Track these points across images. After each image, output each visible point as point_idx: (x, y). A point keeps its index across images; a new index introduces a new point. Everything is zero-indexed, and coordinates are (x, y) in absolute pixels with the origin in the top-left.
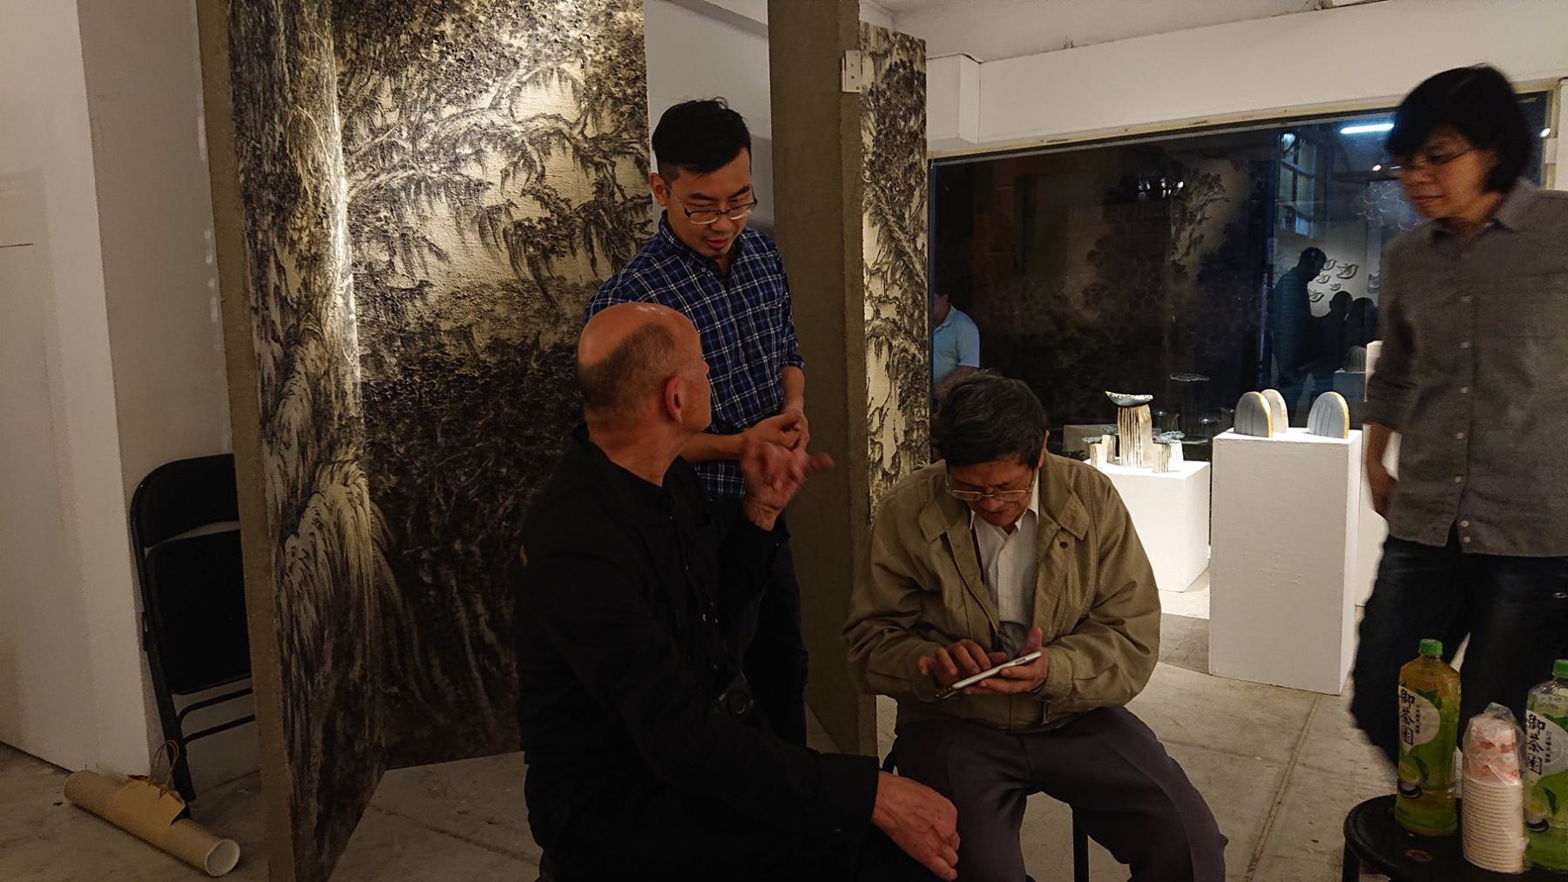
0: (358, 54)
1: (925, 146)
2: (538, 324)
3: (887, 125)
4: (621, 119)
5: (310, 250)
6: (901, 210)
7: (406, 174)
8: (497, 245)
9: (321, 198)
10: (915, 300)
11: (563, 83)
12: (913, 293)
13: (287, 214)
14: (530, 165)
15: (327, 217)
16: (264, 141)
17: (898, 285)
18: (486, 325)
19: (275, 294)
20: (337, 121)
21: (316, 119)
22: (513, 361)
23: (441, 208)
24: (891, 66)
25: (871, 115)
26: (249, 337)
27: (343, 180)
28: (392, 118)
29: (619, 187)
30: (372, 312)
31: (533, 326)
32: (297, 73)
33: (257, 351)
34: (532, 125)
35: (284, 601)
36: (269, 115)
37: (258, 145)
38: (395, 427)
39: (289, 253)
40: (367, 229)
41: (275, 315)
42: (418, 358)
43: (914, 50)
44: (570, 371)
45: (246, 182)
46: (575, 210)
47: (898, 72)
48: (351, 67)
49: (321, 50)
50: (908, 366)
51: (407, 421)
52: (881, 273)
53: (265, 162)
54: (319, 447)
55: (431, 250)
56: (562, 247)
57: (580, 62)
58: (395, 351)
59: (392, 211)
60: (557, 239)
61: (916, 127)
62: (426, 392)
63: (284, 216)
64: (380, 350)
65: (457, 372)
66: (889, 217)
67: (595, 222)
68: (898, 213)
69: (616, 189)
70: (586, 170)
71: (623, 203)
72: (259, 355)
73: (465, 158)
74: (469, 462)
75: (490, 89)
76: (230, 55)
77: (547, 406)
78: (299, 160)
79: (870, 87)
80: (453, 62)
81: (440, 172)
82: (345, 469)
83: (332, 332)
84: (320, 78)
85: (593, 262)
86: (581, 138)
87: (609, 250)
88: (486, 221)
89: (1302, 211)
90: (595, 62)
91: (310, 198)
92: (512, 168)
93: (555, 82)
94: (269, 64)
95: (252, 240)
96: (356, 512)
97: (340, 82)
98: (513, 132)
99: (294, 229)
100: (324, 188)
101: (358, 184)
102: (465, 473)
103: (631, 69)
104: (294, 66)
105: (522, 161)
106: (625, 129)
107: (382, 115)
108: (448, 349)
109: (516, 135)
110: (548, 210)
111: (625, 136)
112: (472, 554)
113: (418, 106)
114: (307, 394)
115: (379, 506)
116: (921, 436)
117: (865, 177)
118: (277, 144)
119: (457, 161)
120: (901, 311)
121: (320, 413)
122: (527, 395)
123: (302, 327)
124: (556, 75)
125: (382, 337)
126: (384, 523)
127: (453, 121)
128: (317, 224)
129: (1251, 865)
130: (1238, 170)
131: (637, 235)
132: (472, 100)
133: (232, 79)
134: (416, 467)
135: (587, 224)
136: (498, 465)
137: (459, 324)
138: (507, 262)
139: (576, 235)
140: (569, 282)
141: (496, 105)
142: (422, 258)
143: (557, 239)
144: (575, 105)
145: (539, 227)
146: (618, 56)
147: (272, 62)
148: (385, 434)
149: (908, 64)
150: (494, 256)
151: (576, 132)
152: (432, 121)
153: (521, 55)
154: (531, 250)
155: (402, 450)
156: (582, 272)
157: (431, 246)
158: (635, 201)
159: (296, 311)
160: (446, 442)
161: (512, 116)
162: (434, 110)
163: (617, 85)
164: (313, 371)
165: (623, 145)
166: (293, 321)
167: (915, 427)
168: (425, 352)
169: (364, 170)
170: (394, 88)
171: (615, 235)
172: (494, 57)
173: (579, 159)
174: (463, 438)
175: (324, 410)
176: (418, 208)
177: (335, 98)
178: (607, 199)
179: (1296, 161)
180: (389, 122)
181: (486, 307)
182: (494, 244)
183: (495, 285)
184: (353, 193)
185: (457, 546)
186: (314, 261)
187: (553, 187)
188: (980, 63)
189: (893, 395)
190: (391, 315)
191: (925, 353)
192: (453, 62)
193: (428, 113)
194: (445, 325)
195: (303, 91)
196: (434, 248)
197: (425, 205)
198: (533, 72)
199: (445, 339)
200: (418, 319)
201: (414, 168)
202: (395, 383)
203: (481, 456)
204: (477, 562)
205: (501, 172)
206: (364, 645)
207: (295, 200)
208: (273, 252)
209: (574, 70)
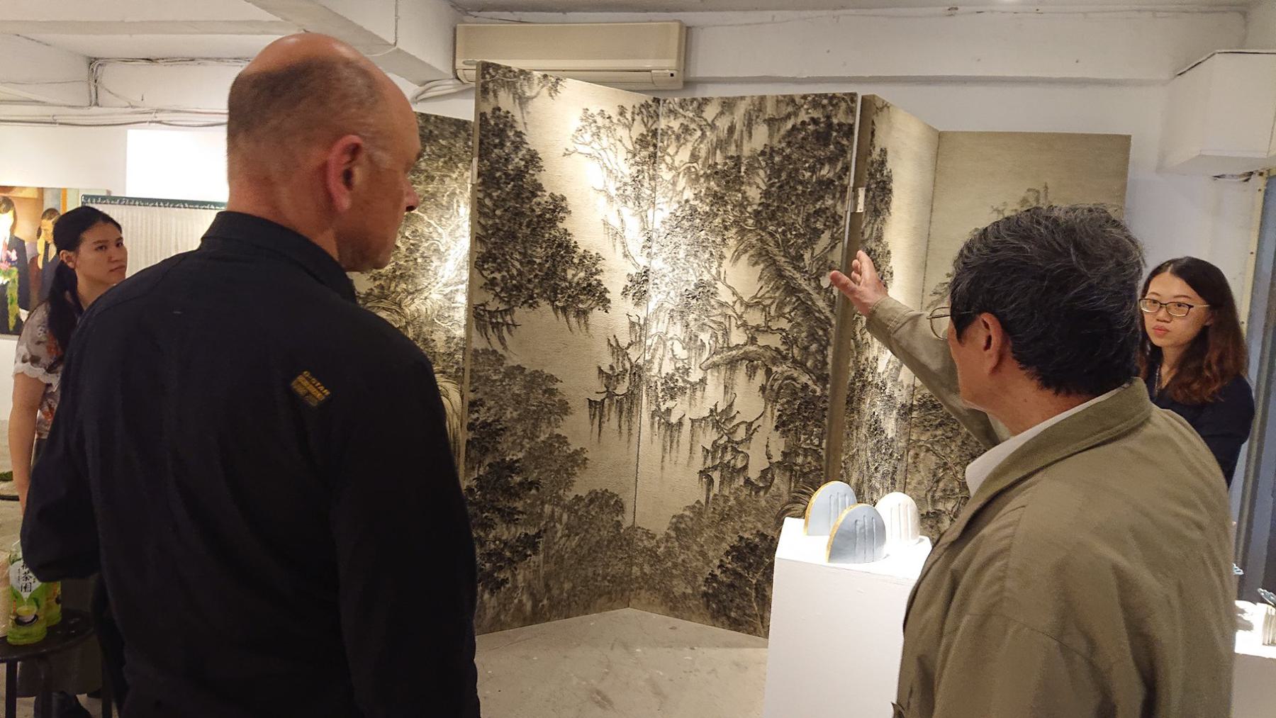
12: (811, 327)
17: (787, 318)
24: (794, 126)
25: (761, 172)
66: (778, 258)
149: (822, 120)
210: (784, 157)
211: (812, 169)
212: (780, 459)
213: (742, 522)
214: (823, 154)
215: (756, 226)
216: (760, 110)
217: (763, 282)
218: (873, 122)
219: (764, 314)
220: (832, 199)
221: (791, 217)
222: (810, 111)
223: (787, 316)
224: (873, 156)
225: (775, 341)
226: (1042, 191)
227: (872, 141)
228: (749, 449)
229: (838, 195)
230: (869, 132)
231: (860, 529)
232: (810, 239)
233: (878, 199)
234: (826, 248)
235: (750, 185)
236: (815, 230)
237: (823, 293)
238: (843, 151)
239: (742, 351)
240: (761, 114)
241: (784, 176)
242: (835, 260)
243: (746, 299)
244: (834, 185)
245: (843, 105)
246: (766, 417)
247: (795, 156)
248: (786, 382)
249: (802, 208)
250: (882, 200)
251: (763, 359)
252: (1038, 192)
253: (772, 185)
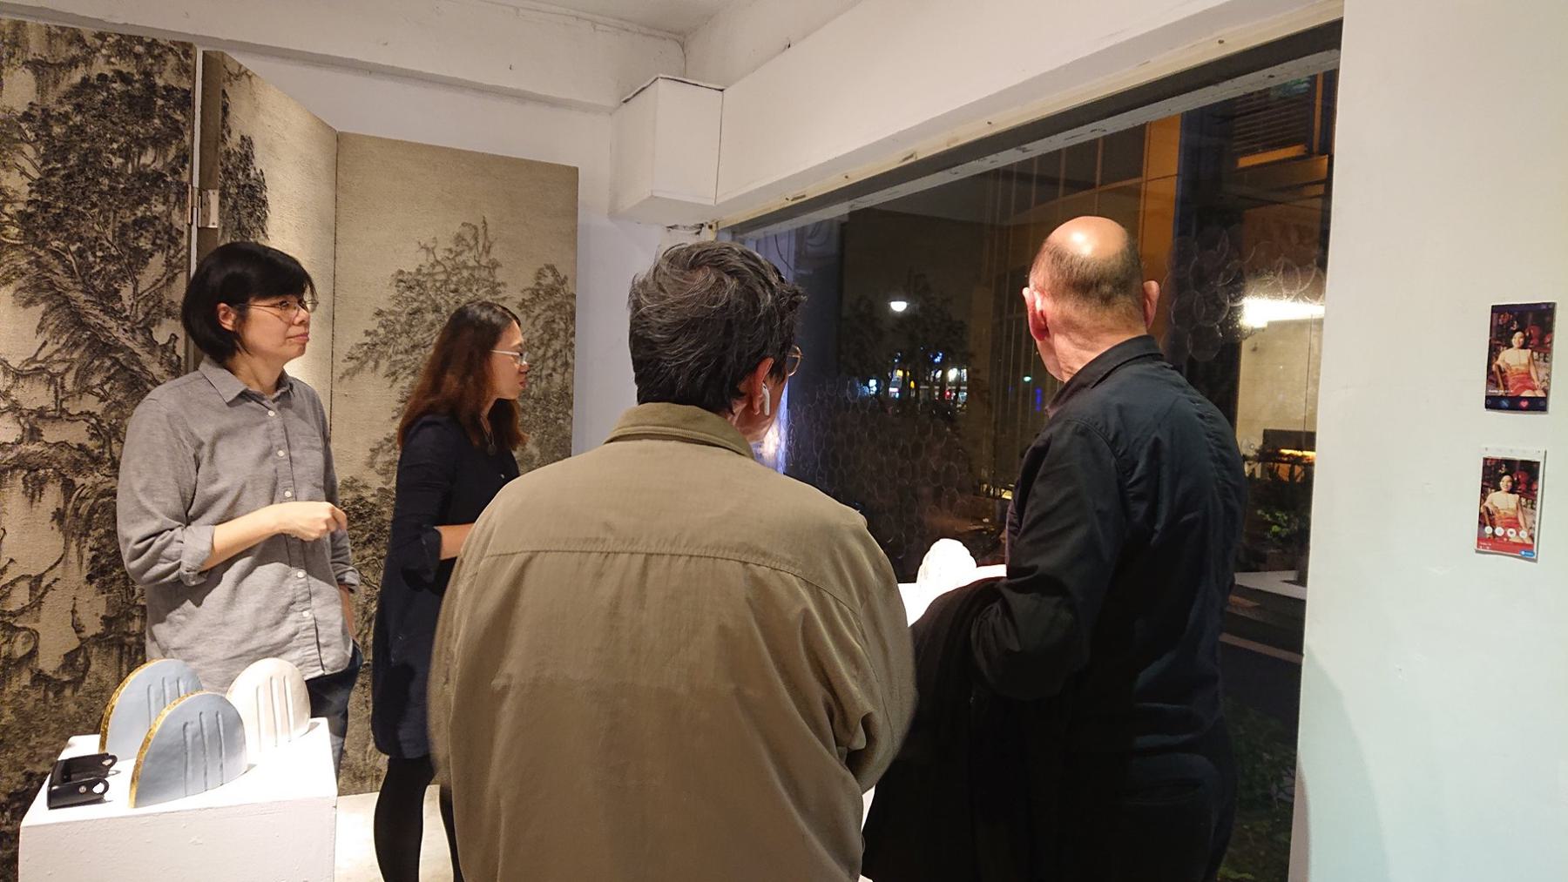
17: (98, 395)
24: (85, 81)
25: (28, 149)
47: (108, 90)
66: (74, 295)
149: (137, 77)
188: (722, 90)
210: (70, 127)
211: (125, 153)
212: (99, 629)
213: (30, 748)
214: (142, 131)
215: (25, 238)
216: (16, 45)
217: (47, 335)
218: (224, 91)
219: (52, 388)
220: (164, 204)
221: (91, 228)
223: (96, 390)
224: (229, 145)
225: (76, 434)
226: (480, 227)
227: (223, 120)
228: (37, 621)
229: (173, 198)
230: (218, 109)
231: (194, 737)
232: (129, 265)
233: (244, 212)
234: (158, 281)
236: (138, 251)
237: (159, 353)
238: (177, 131)
239: (11, 455)
240: (18, 52)
241: (73, 159)
242: (175, 301)
243: (15, 363)
244: (164, 181)
245: (172, 60)
246: (66, 563)
247: (91, 129)
248: (101, 501)
249: (112, 215)
250: (250, 215)
251: (55, 465)
252: (475, 228)
253: (51, 173)
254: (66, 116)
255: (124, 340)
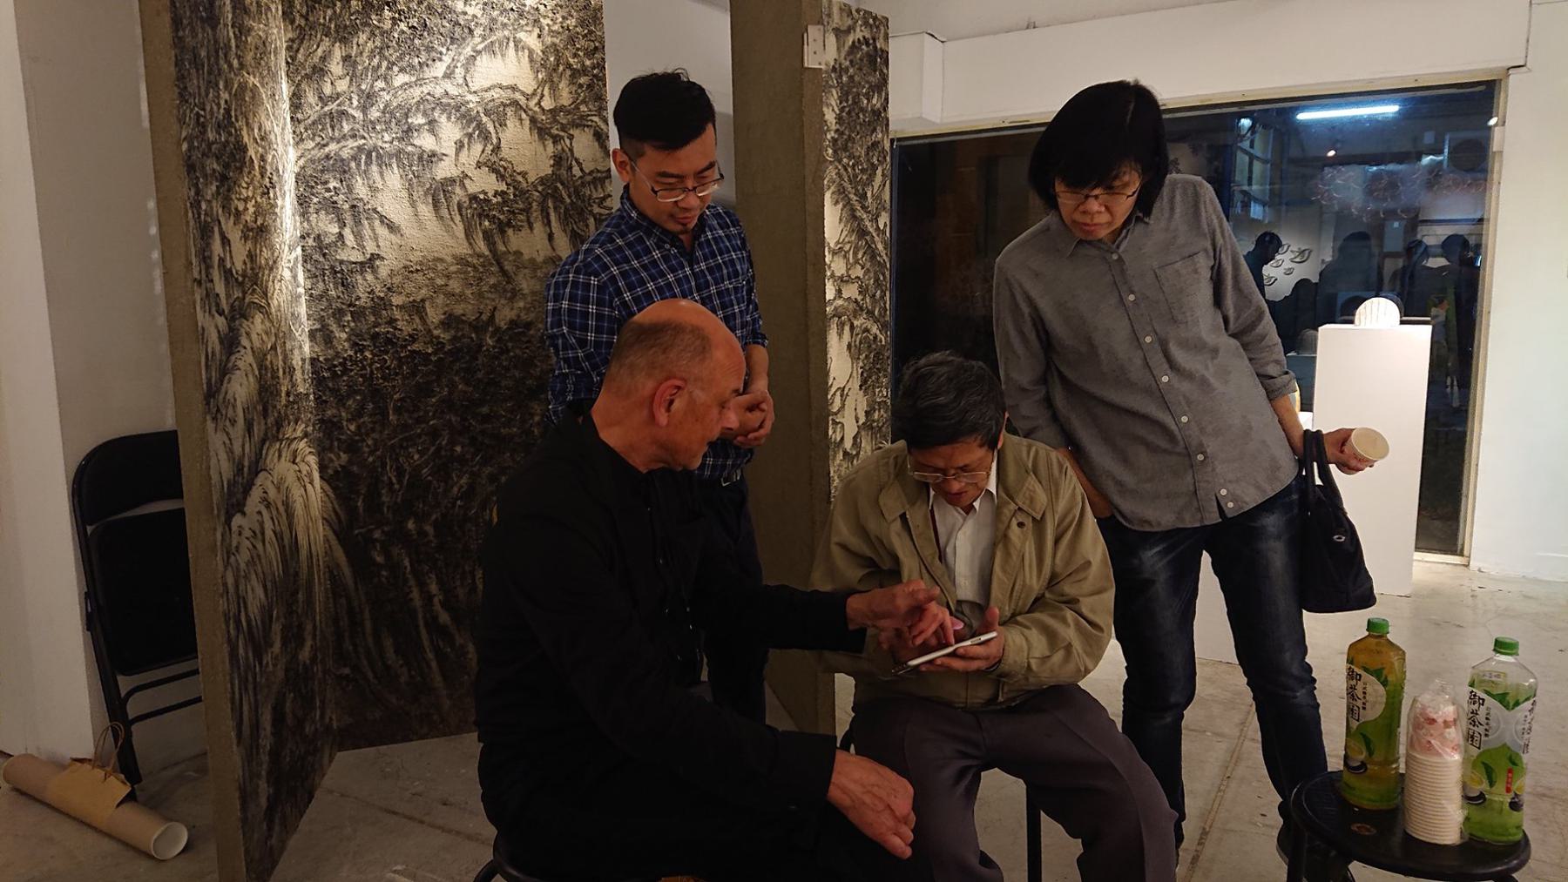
0: (307, 19)
1: (887, 125)
2: (493, 300)
3: (850, 102)
4: (579, 91)
5: (256, 222)
6: (863, 190)
7: (356, 144)
8: (452, 219)
9: (268, 167)
10: (877, 280)
11: (520, 53)
12: (875, 273)
13: (232, 184)
14: (486, 137)
15: (274, 187)
16: (208, 108)
17: (860, 265)
18: (440, 299)
19: (219, 267)
20: (285, 88)
21: (263, 86)
22: (468, 338)
23: (394, 179)
24: (853, 42)
26: (192, 311)
27: (291, 150)
28: (342, 86)
29: (579, 164)
30: (321, 286)
31: (488, 302)
32: (244, 38)
33: (200, 324)
34: (488, 96)
35: (230, 580)
36: (214, 81)
37: (202, 113)
38: (345, 404)
39: (235, 224)
40: (315, 200)
41: (220, 288)
42: (368, 333)
43: (877, 27)
44: (527, 348)
45: (189, 150)
46: (533, 183)
47: (862, 50)
48: (300, 33)
49: (269, 16)
50: (869, 347)
51: (358, 398)
52: (843, 253)
53: (209, 129)
54: (266, 424)
55: (382, 222)
56: (519, 221)
57: (537, 31)
58: (344, 326)
59: (341, 181)
60: (513, 212)
61: (878, 105)
62: (377, 369)
63: (229, 186)
64: (328, 325)
65: (409, 348)
66: (852, 196)
67: (552, 196)
68: (861, 191)
69: (574, 163)
70: (543, 143)
71: (581, 177)
72: (203, 329)
73: (418, 129)
74: (421, 441)
75: (444, 57)
76: (172, 19)
77: (503, 383)
78: (245, 128)
79: (832, 63)
80: (405, 29)
81: (391, 143)
82: (293, 446)
83: (279, 306)
84: (267, 44)
85: (551, 237)
86: (538, 110)
87: (567, 224)
88: (439, 193)
89: (1259, 196)
90: (552, 31)
91: (257, 167)
92: (466, 141)
93: (511, 51)
94: (214, 28)
95: (195, 211)
96: (305, 490)
97: (289, 48)
98: (468, 103)
99: (239, 199)
100: (271, 157)
101: (306, 154)
102: (418, 452)
103: (590, 40)
104: (240, 31)
105: (477, 132)
106: (584, 102)
107: (332, 83)
108: (400, 324)
109: (471, 105)
110: (504, 183)
111: (583, 108)
112: (425, 534)
113: (370, 74)
114: (253, 370)
115: (329, 484)
116: (882, 416)
117: (827, 155)
118: (222, 111)
119: (409, 131)
120: (863, 291)
121: (267, 390)
122: (483, 372)
123: (247, 300)
124: (512, 44)
125: (331, 311)
126: (335, 503)
127: (405, 89)
128: (263, 194)
129: (1201, 838)
130: (1197, 155)
131: (596, 210)
132: (425, 68)
133: (174, 43)
134: (368, 446)
135: (545, 197)
136: (452, 443)
137: (411, 299)
138: (462, 235)
139: (533, 209)
140: (526, 257)
141: (451, 74)
142: (373, 230)
143: (513, 212)
144: (532, 76)
145: (495, 200)
146: (576, 26)
147: (217, 26)
148: (334, 411)
149: (871, 41)
150: (448, 229)
151: (532, 103)
152: (384, 90)
153: (477, 23)
154: (487, 223)
155: (352, 428)
156: (539, 247)
157: (382, 218)
158: (594, 175)
159: (241, 284)
160: (398, 420)
161: (467, 85)
162: (385, 78)
163: (575, 56)
164: (258, 346)
165: (582, 117)
166: (237, 294)
167: (877, 407)
168: (376, 327)
169: (313, 139)
170: (344, 55)
171: (573, 209)
172: (448, 25)
173: (536, 131)
174: (416, 415)
175: (269, 386)
176: (368, 179)
177: (284, 64)
178: (565, 172)
179: (1252, 146)
180: (339, 90)
181: (439, 282)
182: (449, 217)
183: (449, 259)
184: (301, 162)
185: (411, 525)
186: (260, 233)
187: (509, 159)
188: (942, 42)
189: (855, 374)
190: (341, 288)
191: (886, 333)
192: (405, 29)
193: (379, 81)
194: (397, 300)
195: (249, 57)
196: (386, 220)
197: (377, 176)
198: (489, 41)
199: (397, 314)
200: (369, 293)
201: (364, 138)
202: (345, 359)
203: (434, 434)
204: (431, 541)
205: (456, 143)
206: (315, 627)
207: (241, 170)
208: (217, 223)
209: (531, 39)
222: (863, 28)
232: (870, 175)
235: (828, 105)
247: (857, 78)
254: (847, 70)
255: (869, 227)
